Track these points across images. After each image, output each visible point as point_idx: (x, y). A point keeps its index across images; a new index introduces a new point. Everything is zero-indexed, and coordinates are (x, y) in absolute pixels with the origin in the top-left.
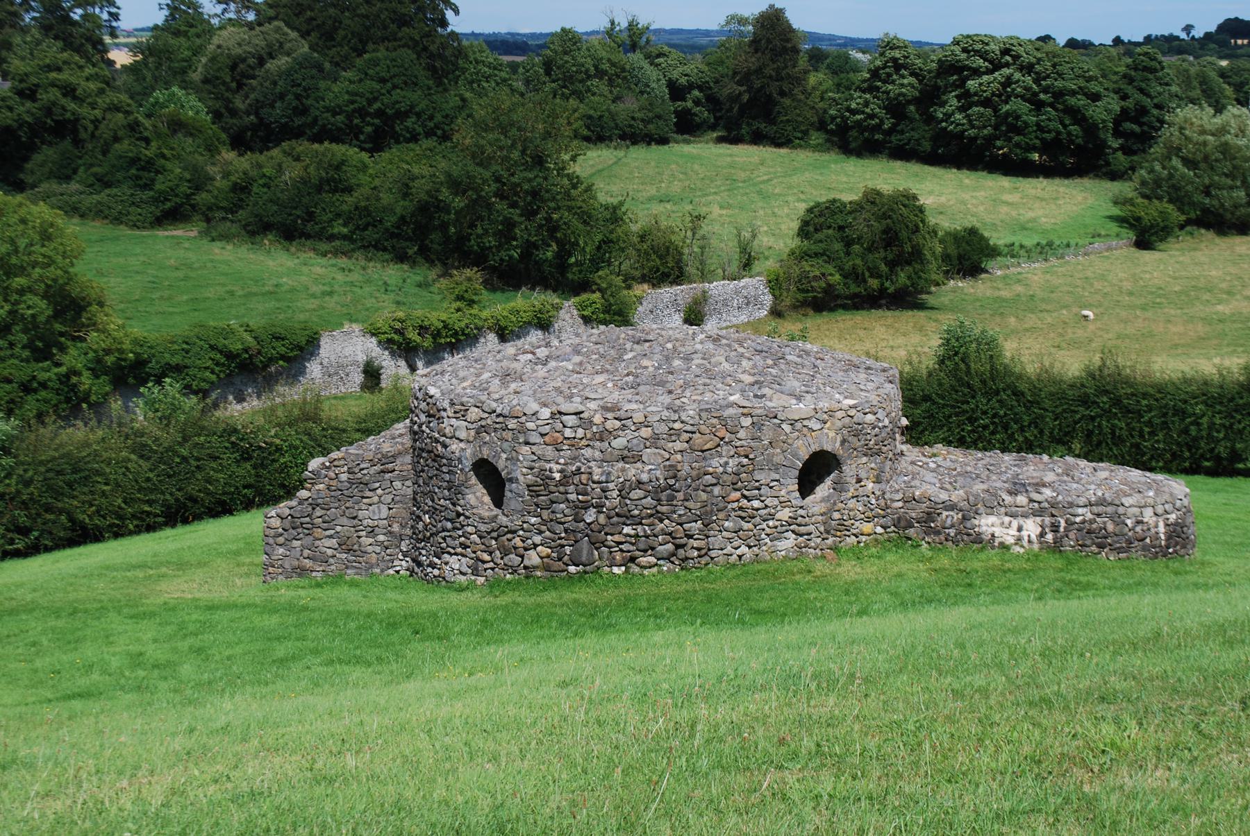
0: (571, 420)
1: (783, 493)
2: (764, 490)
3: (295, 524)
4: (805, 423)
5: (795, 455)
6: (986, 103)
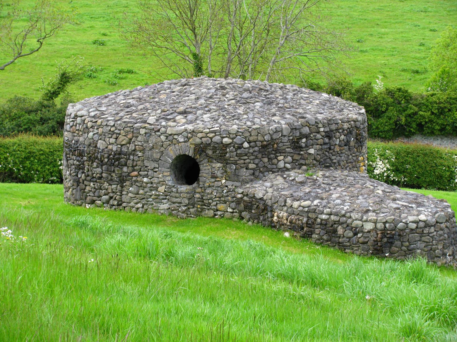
1: (160, 176)
2: (150, 173)
4: (176, 137)
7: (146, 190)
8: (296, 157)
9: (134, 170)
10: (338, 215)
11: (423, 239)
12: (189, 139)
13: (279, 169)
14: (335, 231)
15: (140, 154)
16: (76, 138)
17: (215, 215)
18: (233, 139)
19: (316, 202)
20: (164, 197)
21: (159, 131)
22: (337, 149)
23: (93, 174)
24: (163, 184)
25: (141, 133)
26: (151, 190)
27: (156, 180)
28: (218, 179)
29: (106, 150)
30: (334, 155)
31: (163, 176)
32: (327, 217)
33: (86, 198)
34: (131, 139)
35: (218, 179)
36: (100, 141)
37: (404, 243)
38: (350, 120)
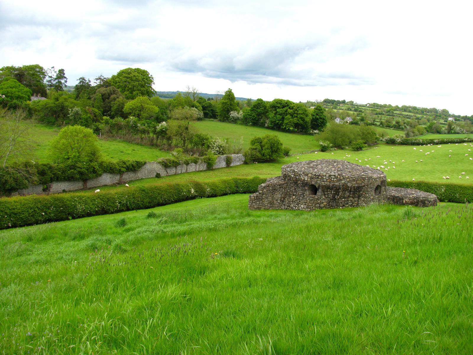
0: (333, 177)
2: (369, 192)
3: (257, 198)
6: (280, 114)
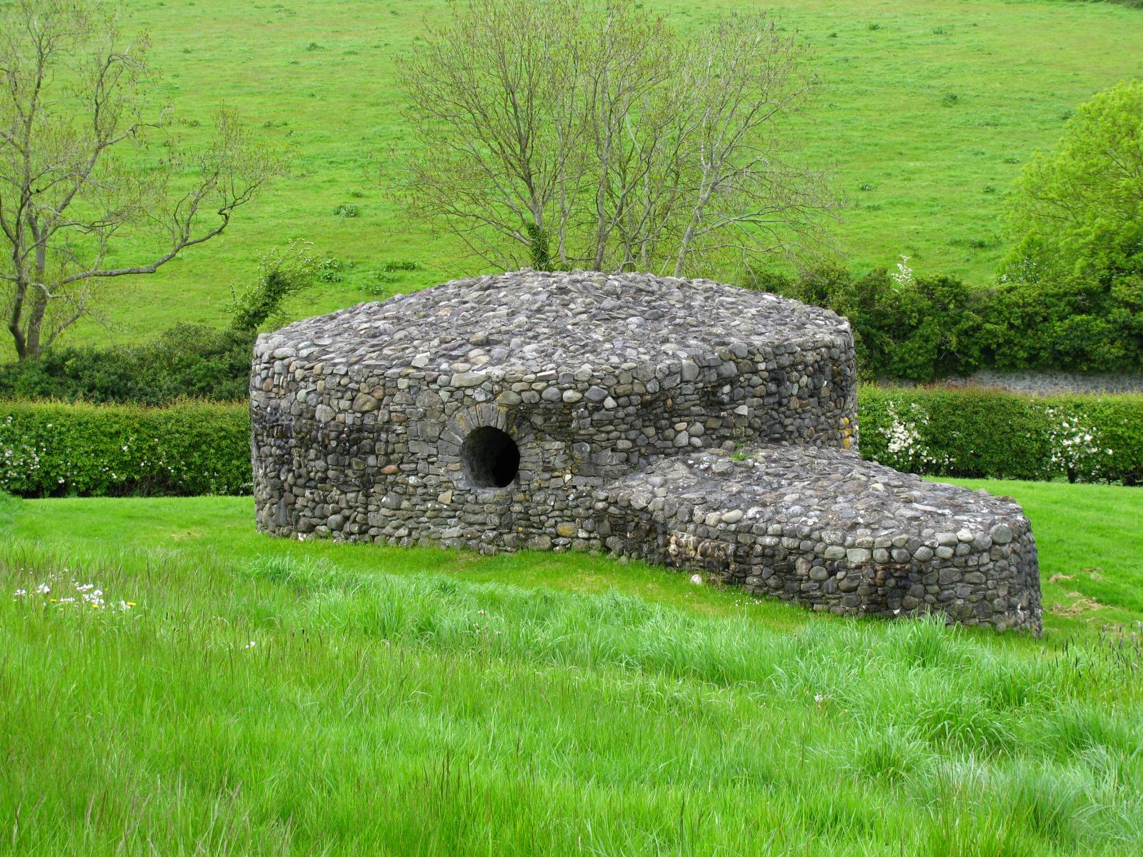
1: (442, 471)
2: (421, 465)
4: (469, 392)
5: (454, 428)
7: (414, 500)
8: (713, 423)
9: (389, 462)
10: (795, 537)
11: (968, 577)
12: (495, 395)
13: (679, 448)
14: (792, 568)
15: (400, 429)
16: (273, 402)
17: (554, 545)
18: (583, 391)
19: (752, 512)
20: (452, 514)
21: (435, 381)
22: (795, 403)
23: (309, 472)
24: (448, 488)
25: (399, 386)
26: (425, 501)
27: (433, 480)
28: (557, 474)
29: (333, 423)
30: (789, 417)
31: (447, 471)
32: (775, 540)
33: (297, 522)
34: (381, 400)
35: (557, 474)
36: (319, 406)
37: (929, 588)
38: (819, 344)
